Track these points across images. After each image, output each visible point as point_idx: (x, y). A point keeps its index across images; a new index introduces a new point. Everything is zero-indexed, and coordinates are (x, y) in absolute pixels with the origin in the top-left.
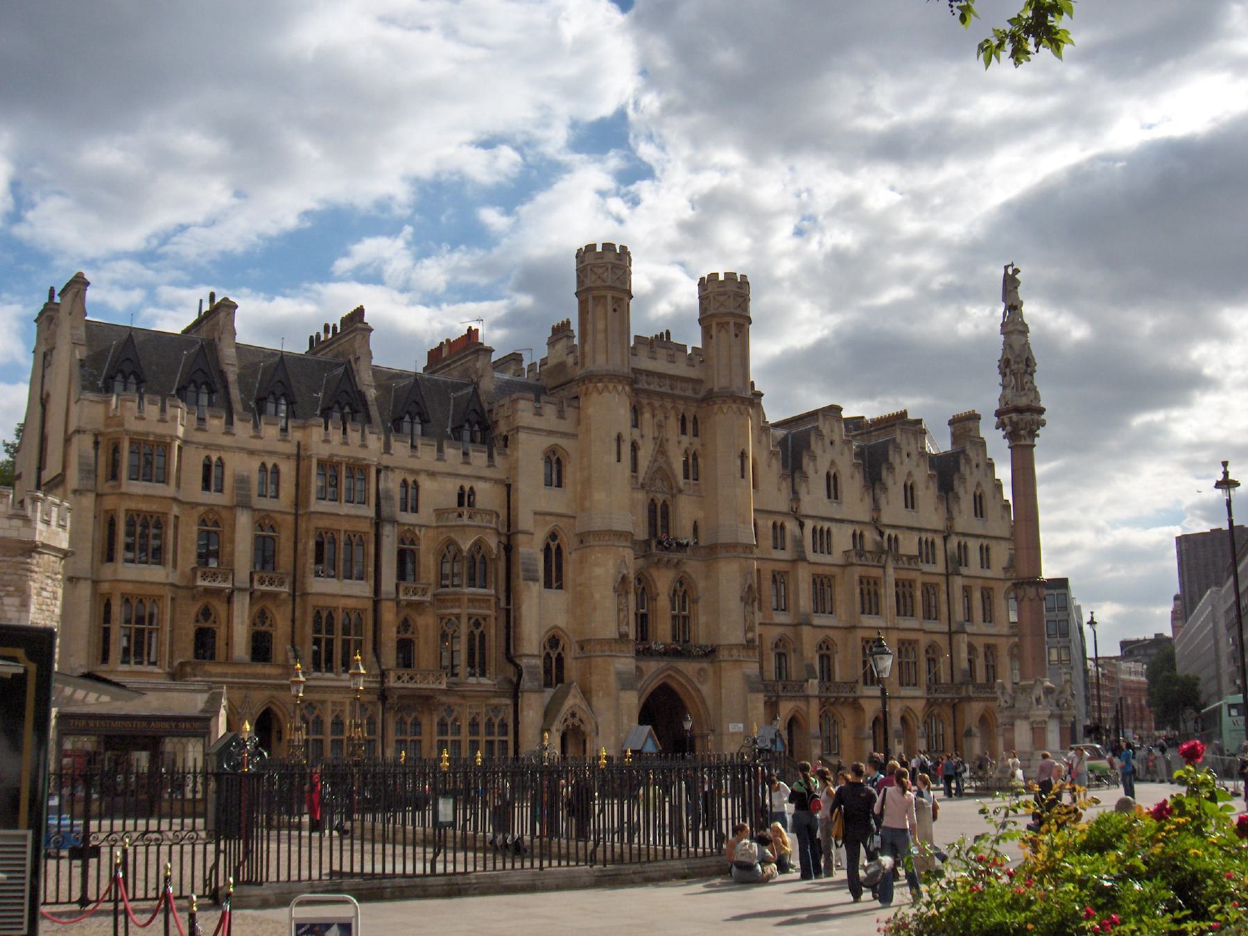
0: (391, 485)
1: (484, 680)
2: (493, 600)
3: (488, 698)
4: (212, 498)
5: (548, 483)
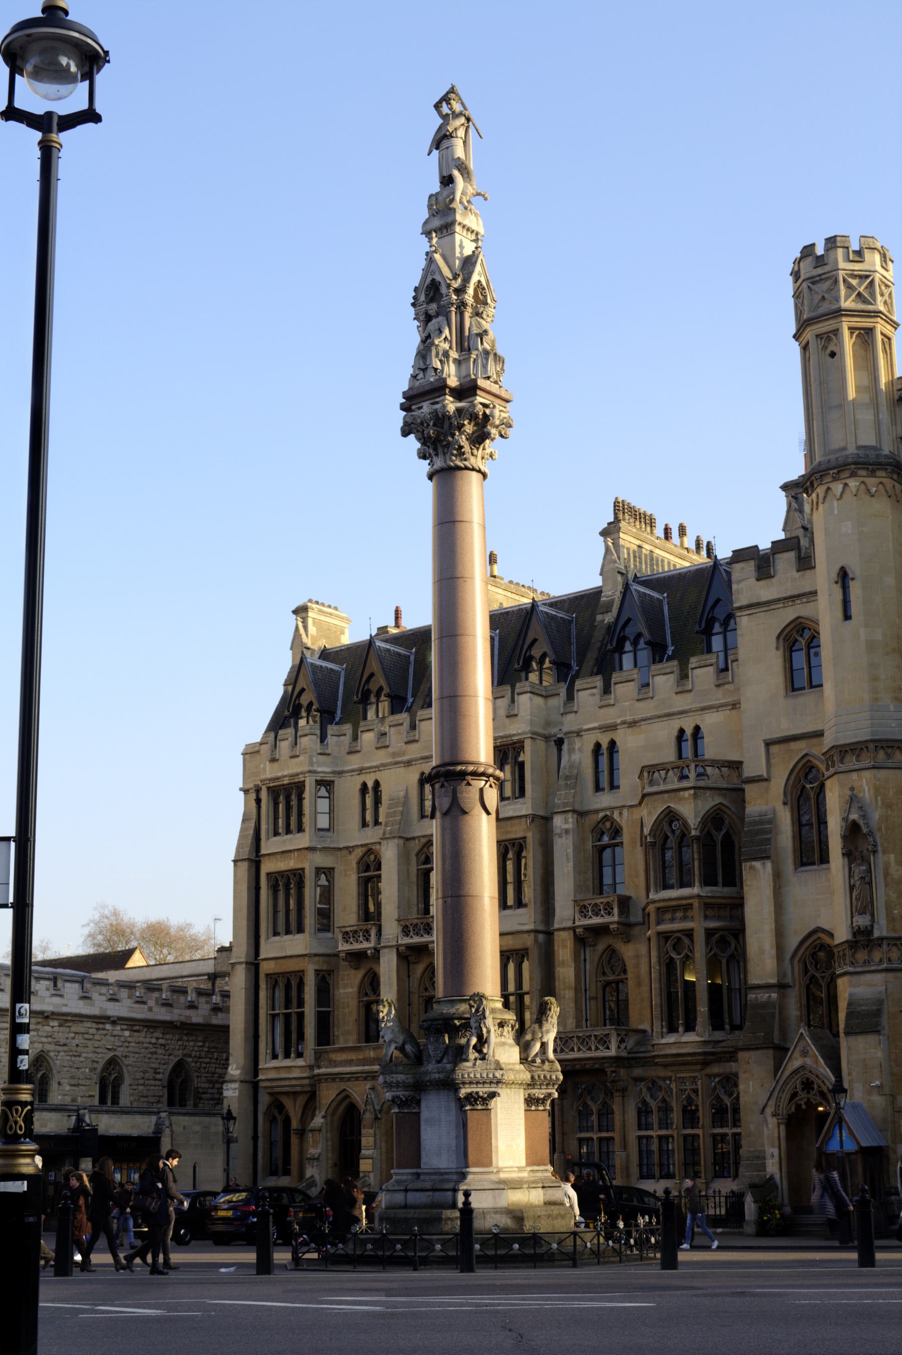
0: (576, 757)
1: (691, 1037)
2: (696, 903)
3: (706, 1064)
4: (371, 835)
5: (793, 687)
